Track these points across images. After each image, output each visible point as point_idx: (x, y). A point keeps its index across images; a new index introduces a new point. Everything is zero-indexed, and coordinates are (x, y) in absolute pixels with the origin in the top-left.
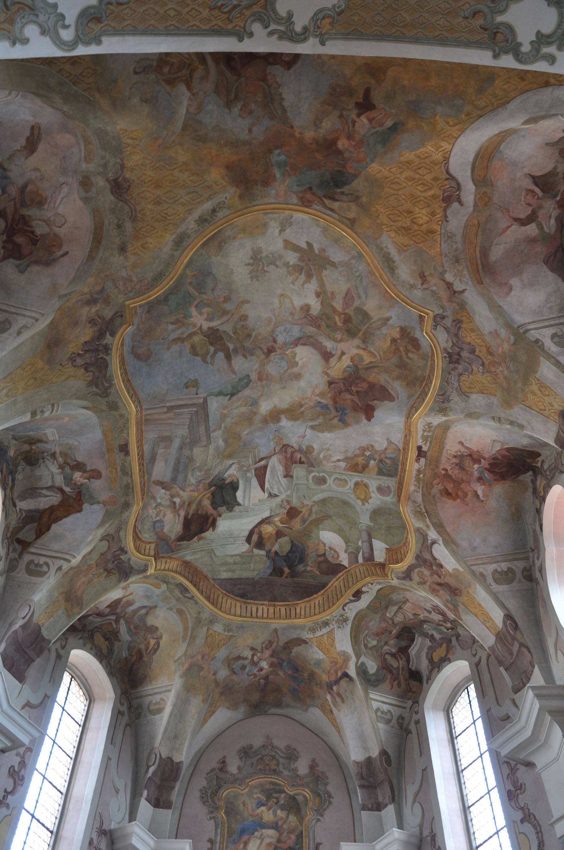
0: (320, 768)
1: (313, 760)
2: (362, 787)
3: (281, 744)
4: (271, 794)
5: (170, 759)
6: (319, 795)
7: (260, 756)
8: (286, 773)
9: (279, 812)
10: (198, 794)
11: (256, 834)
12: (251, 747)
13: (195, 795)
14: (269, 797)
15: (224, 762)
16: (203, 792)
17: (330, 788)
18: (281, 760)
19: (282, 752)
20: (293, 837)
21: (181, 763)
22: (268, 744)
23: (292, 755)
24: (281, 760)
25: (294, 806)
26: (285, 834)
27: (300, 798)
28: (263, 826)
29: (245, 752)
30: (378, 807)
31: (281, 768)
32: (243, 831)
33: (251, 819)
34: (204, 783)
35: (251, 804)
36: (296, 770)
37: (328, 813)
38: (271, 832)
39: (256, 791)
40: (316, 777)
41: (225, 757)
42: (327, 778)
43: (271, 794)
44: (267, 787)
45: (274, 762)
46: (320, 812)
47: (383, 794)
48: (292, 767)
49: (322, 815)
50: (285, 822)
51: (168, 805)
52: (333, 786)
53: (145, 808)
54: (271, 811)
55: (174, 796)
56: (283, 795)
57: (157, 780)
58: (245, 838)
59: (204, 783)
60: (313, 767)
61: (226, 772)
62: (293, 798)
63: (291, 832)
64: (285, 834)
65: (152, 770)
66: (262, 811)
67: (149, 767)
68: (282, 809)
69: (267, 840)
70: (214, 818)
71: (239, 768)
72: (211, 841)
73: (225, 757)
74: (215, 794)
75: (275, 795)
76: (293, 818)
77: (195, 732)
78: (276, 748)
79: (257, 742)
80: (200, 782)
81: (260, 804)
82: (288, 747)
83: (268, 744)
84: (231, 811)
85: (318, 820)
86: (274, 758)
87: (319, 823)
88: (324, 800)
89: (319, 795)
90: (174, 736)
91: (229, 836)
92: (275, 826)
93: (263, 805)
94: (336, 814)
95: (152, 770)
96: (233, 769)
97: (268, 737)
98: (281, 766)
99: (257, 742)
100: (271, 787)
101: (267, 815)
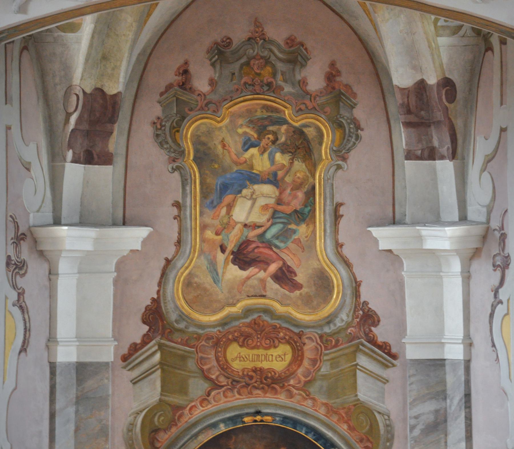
0: (344, 78)
1: (333, 65)
2: (408, 124)
3: (277, 34)
4: (264, 126)
5: (100, 91)
6: (340, 126)
7: (243, 61)
8: (288, 89)
9: (278, 156)
10: (149, 130)
11: (245, 192)
12: (228, 42)
13: (145, 132)
14: (262, 131)
15: (186, 72)
16: (158, 125)
17: (359, 113)
18: (280, 66)
19: (281, 52)
20: (300, 195)
21: (120, 93)
22: (258, 37)
23: (296, 55)
24: (280, 66)
25: (301, 146)
26: (288, 191)
27: (310, 132)
28: (255, 179)
29: (221, 53)
30: (432, 155)
31: (279, 80)
32: (224, 189)
33: (235, 169)
34: (158, 111)
35: (234, 144)
36: (303, 83)
37: (353, 155)
38: (267, 189)
39: (240, 121)
40: (337, 96)
41: (186, 63)
42: (355, 95)
43: (265, 127)
44: (259, 114)
45: (269, 69)
46: (341, 153)
47: (439, 139)
48: (298, 77)
49: (344, 159)
50: (287, 172)
51: (107, 159)
52: (364, 110)
53: (74, 173)
54: (266, 155)
55: (116, 143)
56: (284, 128)
57: (85, 126)
58: (228, 198)
59: (158, 111)
60: (331, 76)
61: (191, 90)
62: (299, 133)
63: (297, 187)
64: (288, 191)
65: (73, 119)
66: (252, 156)
67: (68, 115)
68: (283, 152)
69: (261, 202)
70: (178, 168)
71: (212, 83)
72: (177, 205)
73: (186, 63)
74: (176, 128)
75: (271, 128)
76: (299, 166)
77: (135, 41)
78: (271, 42)
79: (239, 34)
80: (151, 109)
81: (248, 144)
82: (291, 41)
83: (258, 37)
84: (204, 157)
85: (339, 167)
86: (267, 62)
87: (340, 172)
88: (349, 134)
89: (340, 126)
90: (101, 56)
91: (205, 195)
92: (273, 179)
93: (253, 146)
94: (368, 156)
95: (73, 119)
96: (201, 84)
97: (257, 23)
98: (279, 77)
99: (239, 34)
100: (266, 114)
101: (261, 163)
